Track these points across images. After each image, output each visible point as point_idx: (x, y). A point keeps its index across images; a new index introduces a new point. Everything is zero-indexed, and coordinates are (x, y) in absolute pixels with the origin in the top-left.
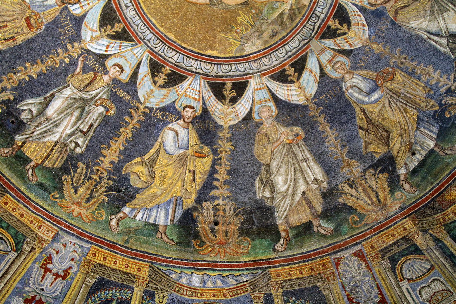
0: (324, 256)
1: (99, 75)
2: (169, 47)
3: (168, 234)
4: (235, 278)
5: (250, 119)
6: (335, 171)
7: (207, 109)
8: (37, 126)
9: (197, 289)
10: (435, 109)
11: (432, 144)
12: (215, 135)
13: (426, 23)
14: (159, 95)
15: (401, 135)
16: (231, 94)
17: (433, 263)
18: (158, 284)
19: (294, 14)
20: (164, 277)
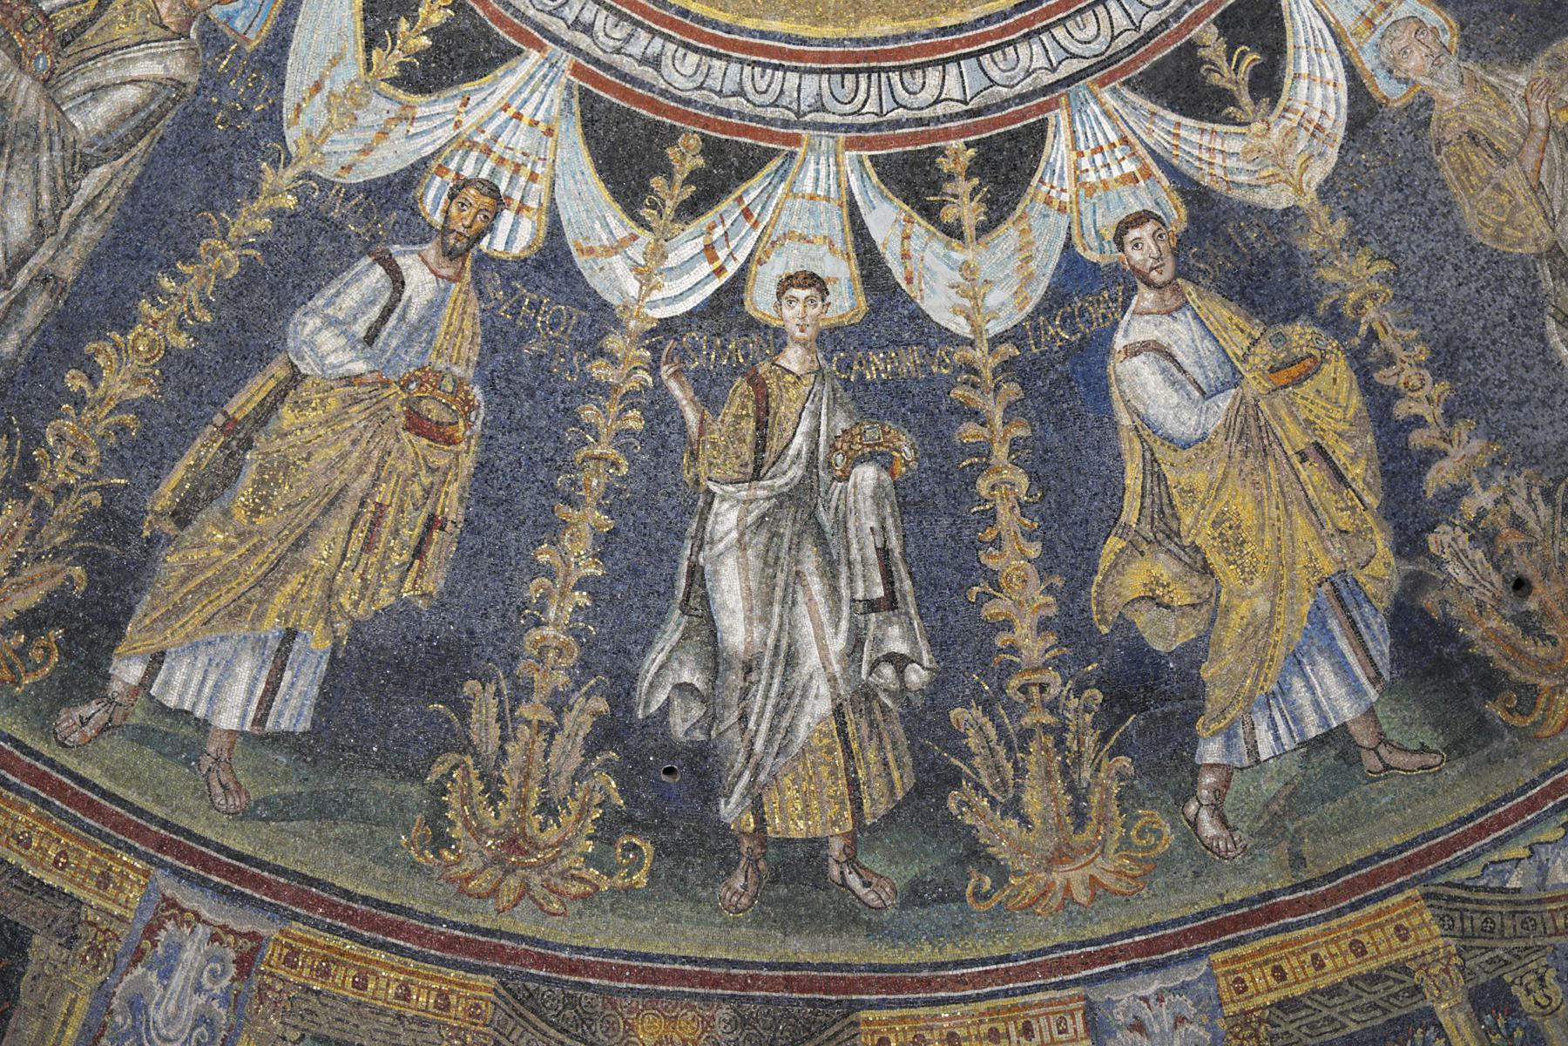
1: (763, 368)
2: (901, 69)
3: (1394, 736)
5: (1373, 113)
7: (1197, 184)
8: (743, 718)
12: (1290, 258)
14: (1002, 264)
16: (1243, 68)
18: (1492, 943)
20: (1492, 903)
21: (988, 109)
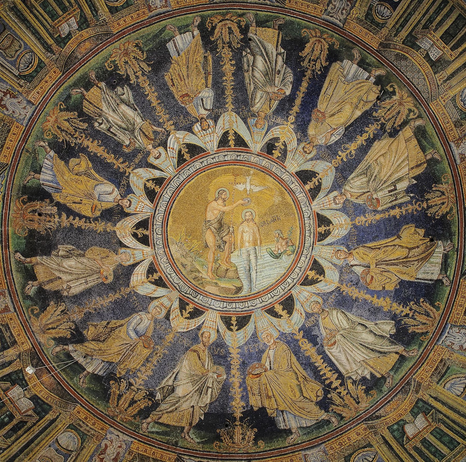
0: (8, 285)
5: (121, 246)
6: (75, 302)
8: (112, 98)
11: (90, 369)
13: (186, 371)
19: (199, 280)
21: (160, 198)
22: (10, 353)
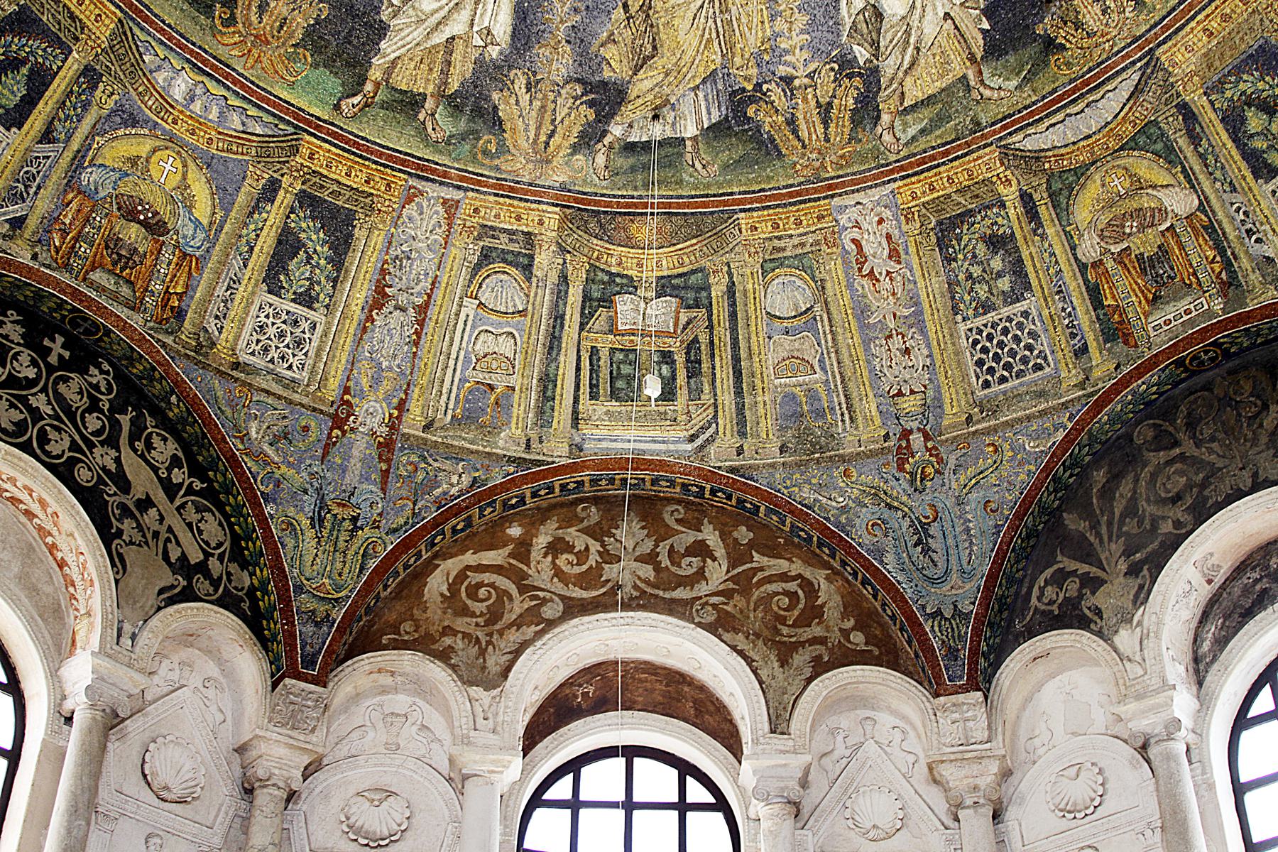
4: (243, 118)
9: (172, 106)
10: (746, 84)
11: (690, 131)
15: (667, 75)
17: (530, 308)
22: (545, 263)
